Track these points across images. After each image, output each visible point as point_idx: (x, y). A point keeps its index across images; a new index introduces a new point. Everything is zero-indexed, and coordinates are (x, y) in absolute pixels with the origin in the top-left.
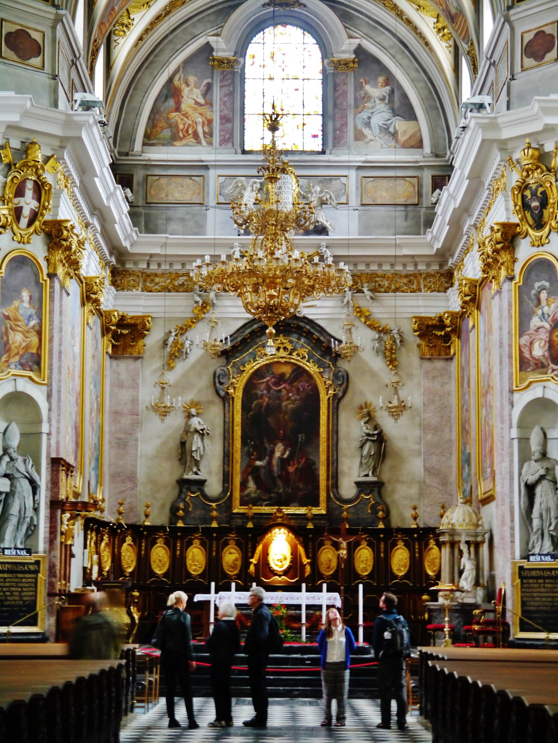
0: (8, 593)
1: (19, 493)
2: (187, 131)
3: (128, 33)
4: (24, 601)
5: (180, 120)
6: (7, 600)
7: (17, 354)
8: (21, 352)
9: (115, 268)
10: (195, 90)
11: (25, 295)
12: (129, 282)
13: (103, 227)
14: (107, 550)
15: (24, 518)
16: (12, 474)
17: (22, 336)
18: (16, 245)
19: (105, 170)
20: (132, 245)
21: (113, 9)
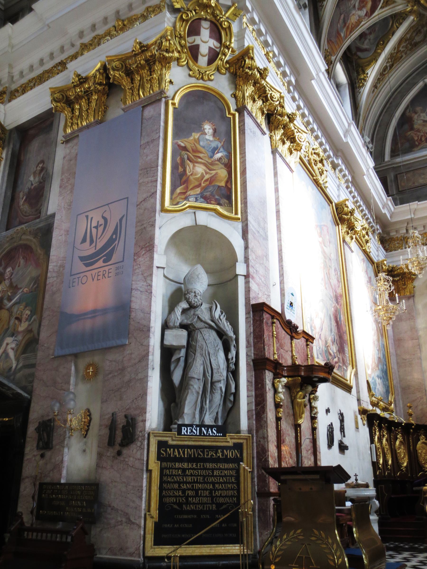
0: (190, 493)
1: (202, 349)
2: (421, 139)
3: (365, 84)
4: (219, 505)
5: (414, 135)
6: (188, 503)
7: (199, 186)
8: (203, 185)
9: (383, 237)
10: (422, 114)
11: (208, 128)
12: (395, 245)
13: (353, 177)
14: (402, 447)
15: (212, 383)
16: (192, 324)
17: (204, 168)
18: (193, 80)
19: (321, 75)
20: (390, 217)
21: (338, 33)
